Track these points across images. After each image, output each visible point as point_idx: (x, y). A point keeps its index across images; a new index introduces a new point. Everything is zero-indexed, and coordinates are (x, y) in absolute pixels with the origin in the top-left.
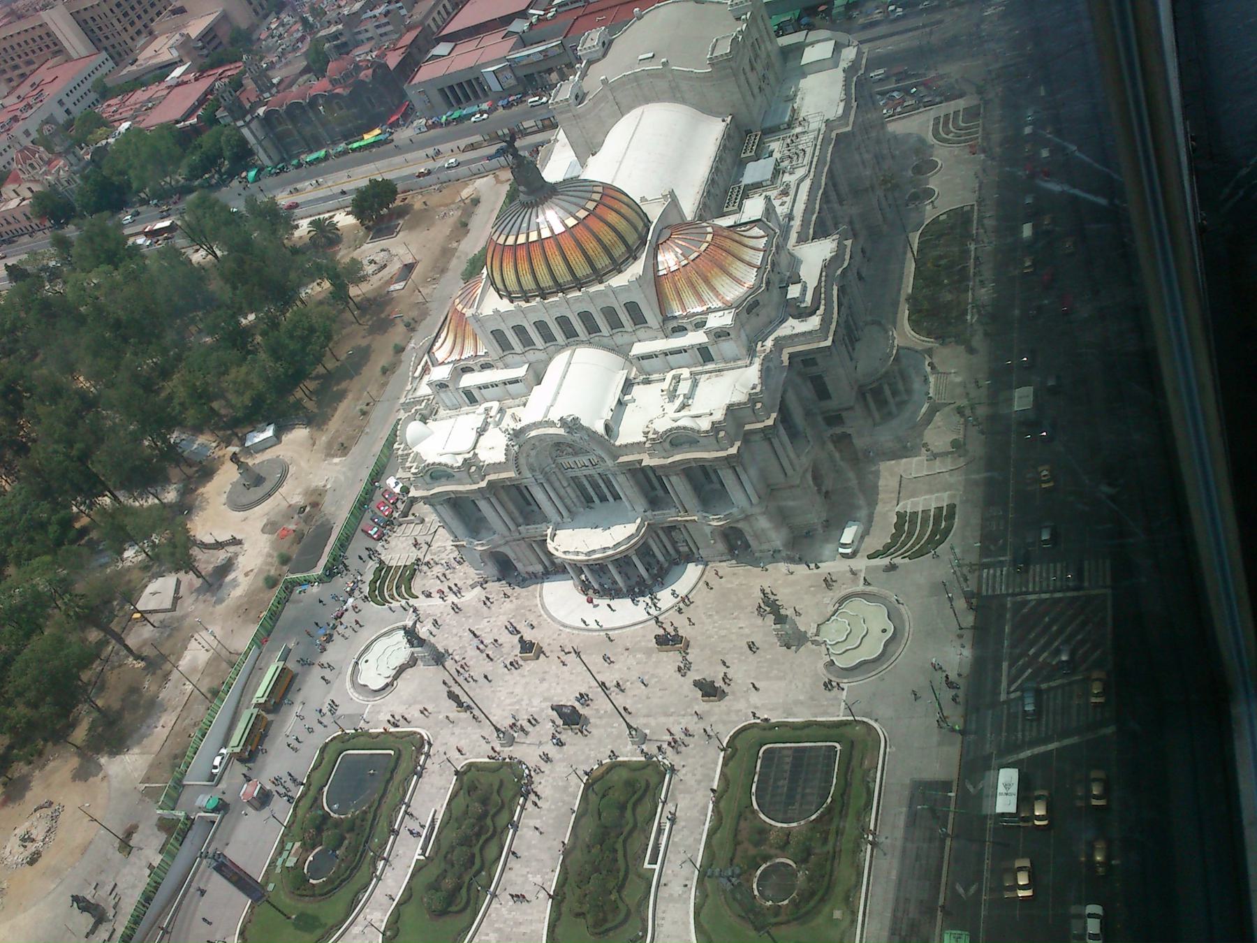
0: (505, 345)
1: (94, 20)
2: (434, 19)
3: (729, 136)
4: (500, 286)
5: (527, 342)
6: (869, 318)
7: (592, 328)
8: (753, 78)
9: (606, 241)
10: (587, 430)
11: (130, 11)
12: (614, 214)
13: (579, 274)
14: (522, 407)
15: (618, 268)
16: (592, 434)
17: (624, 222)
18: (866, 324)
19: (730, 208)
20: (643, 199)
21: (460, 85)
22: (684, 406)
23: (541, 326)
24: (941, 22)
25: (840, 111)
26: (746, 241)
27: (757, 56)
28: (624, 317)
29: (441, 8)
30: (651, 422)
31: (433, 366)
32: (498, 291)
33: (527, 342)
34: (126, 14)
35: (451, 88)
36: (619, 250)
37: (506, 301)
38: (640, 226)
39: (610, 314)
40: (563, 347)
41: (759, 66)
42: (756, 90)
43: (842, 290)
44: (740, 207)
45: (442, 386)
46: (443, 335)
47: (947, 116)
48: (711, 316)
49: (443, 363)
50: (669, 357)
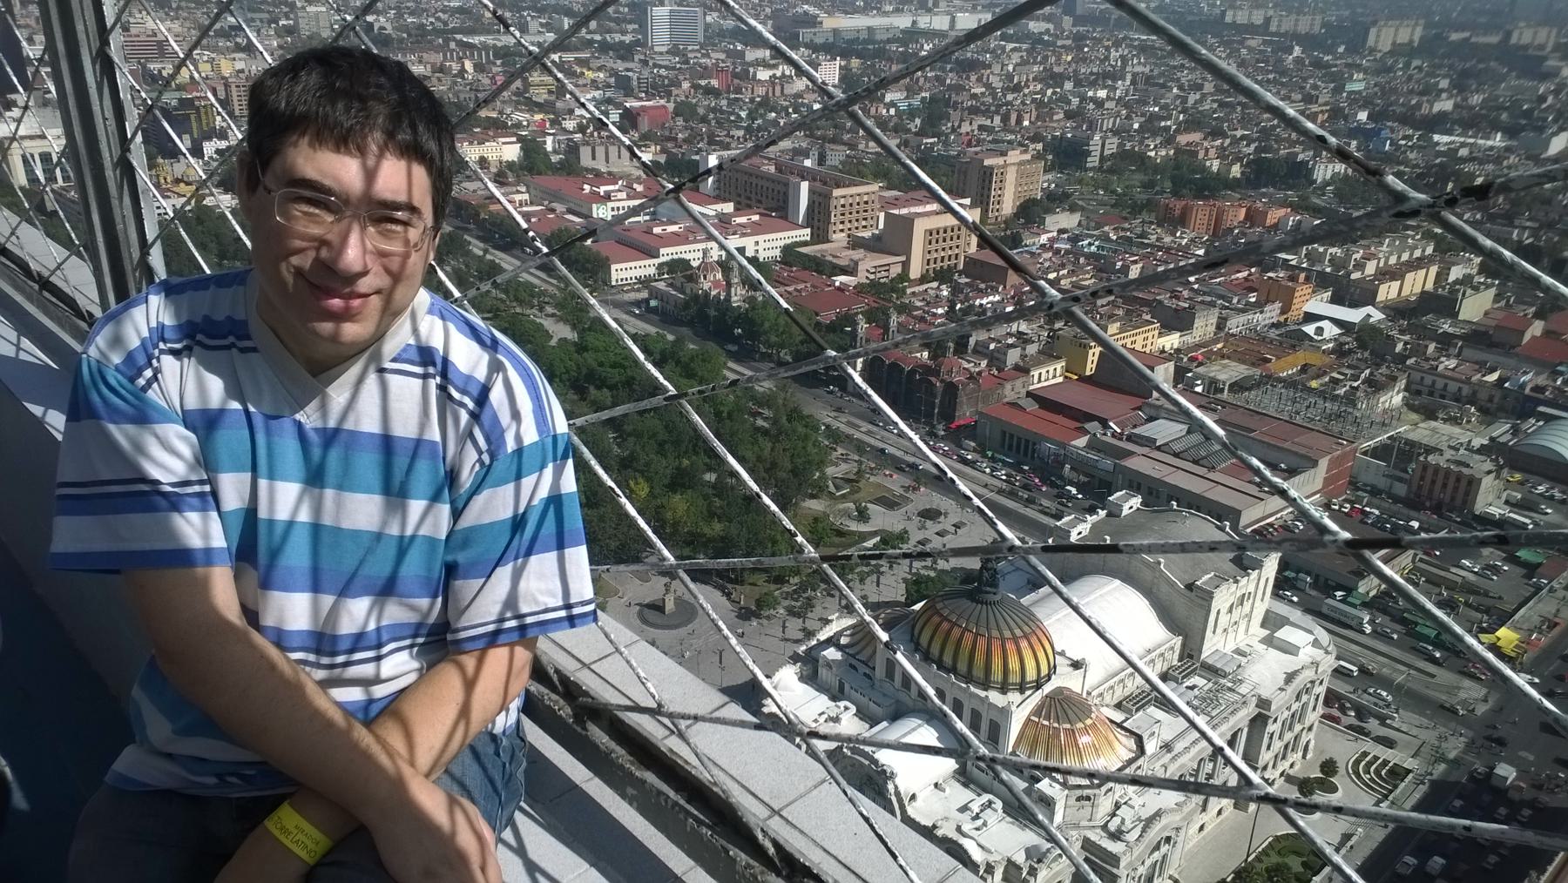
3: (1172, 648)
6: (1177, 876)
10: (896, 787)
12: (1030, 651)
15: (1004, 689)
16: (897, 794)
17: (1033, 663)
18: (1170, 877)
19: (1129, 706)
20: (1062, 654)
21: (1019, 439)
22: (977, 829)
24: (1433, 676)
26: (1116, 744)
28: (984, 726)
29: (1051, 369)
30: (946, 819)
32: (912, 635)
38: (1044, 670)
43: (1168, 839)
44: (1137, 710)
47: (1376, 758)
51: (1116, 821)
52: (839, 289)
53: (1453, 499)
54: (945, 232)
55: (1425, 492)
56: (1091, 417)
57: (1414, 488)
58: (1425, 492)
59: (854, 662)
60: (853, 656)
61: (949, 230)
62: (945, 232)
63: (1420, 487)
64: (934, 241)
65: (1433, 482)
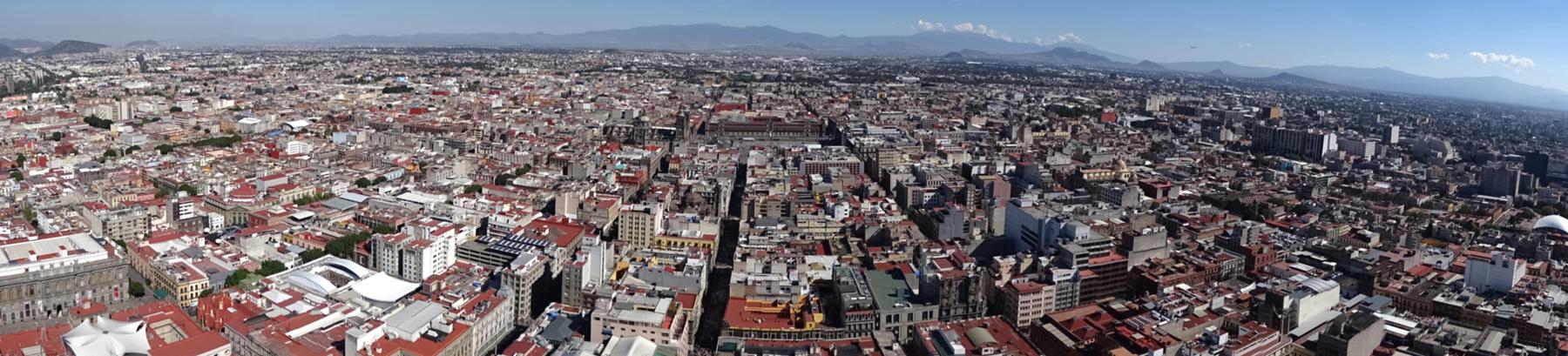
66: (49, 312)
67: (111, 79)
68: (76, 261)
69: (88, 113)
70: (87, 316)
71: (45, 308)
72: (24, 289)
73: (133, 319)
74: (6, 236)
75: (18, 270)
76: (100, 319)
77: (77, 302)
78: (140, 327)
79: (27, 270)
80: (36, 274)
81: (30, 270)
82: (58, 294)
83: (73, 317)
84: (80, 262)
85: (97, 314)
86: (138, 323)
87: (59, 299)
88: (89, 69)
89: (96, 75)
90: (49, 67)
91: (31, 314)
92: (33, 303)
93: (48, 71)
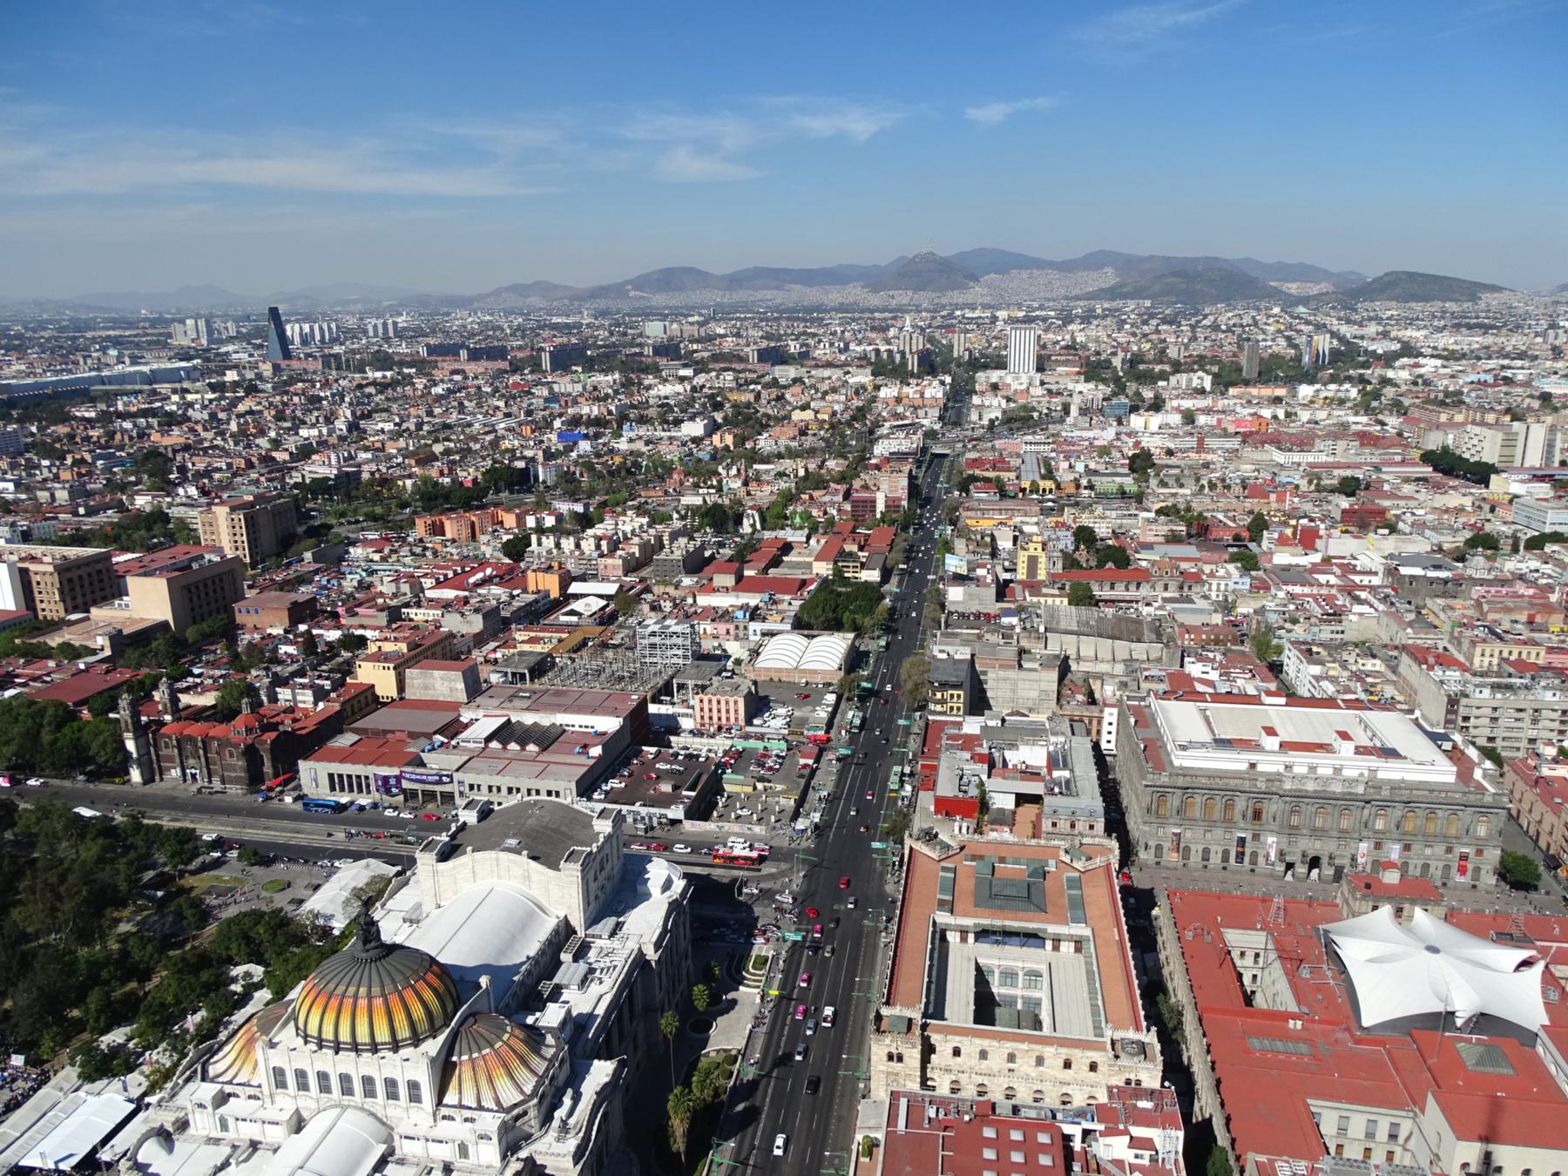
0: (281, 1083)
1: (38, 583)
2: (352, 706)
4: (301, 1025)
5: (303, 1086)
7: (370, 1092)
8: (593, 886)
9: (415, 1016)
11: (78, 588)
13: (379, 1039)
14: (270, 1153)
15: (416, 1041)
21: (349, 777)
23: (323, 1077)
25: (654, 939)
27: (602, 869)
28: (403, 1091)
31: (203, 1080)
32: (297, 1029)
33: (303, 1086)
34: (72, 590)
35: (340, 776)
36: (423, 1026)
37: (300, 1041)
39: (391, 1084)
40: (335, 1106)
41: (602, 876)
42: (592, 898)
45: (201, 1106)
46: (227, 1049)
48: (484, 1114)
49: (212, 1081)
50: (430, 1144)
51: (556, 1123)
52: (87, 670)
53: (728, 719)
54: (206, 585)
55: (707, 720)
56: (414, 736)
57: (699, 720)
58: (707, 720)
59: (228, 1089)
60: (230, 1082)
61: (210, 583)
62: (206, 585)
63: (702, 717)
64: (195, 598)
65: (710, 710)
66: (1290, 866)
67: (1503, 367)
68: (1373, 771)
69: (1433, 441)
70: (1389, 899)
71: (1281, 854)
72: (1241, 803)
73: (1506, 938)
74: (1210, 683)
75: (1233, 762)
76: (1420, 916)
77: (1360, 860)
78: (1526, 963)
79: (1253, 766)
80: (1273, 778)
81: (1260, 768)
82: (1317, 833)
83: (1352, 891)
84: (1381, 775)
85: (1414, 902)
86: (1524, 954)
87: (1318, 845)
88: (1446, 341)
89: (1464, 356)
90: (1346, 330)
91: (1247, 859)
92: (1256, 837)
93: (1342, 339)
